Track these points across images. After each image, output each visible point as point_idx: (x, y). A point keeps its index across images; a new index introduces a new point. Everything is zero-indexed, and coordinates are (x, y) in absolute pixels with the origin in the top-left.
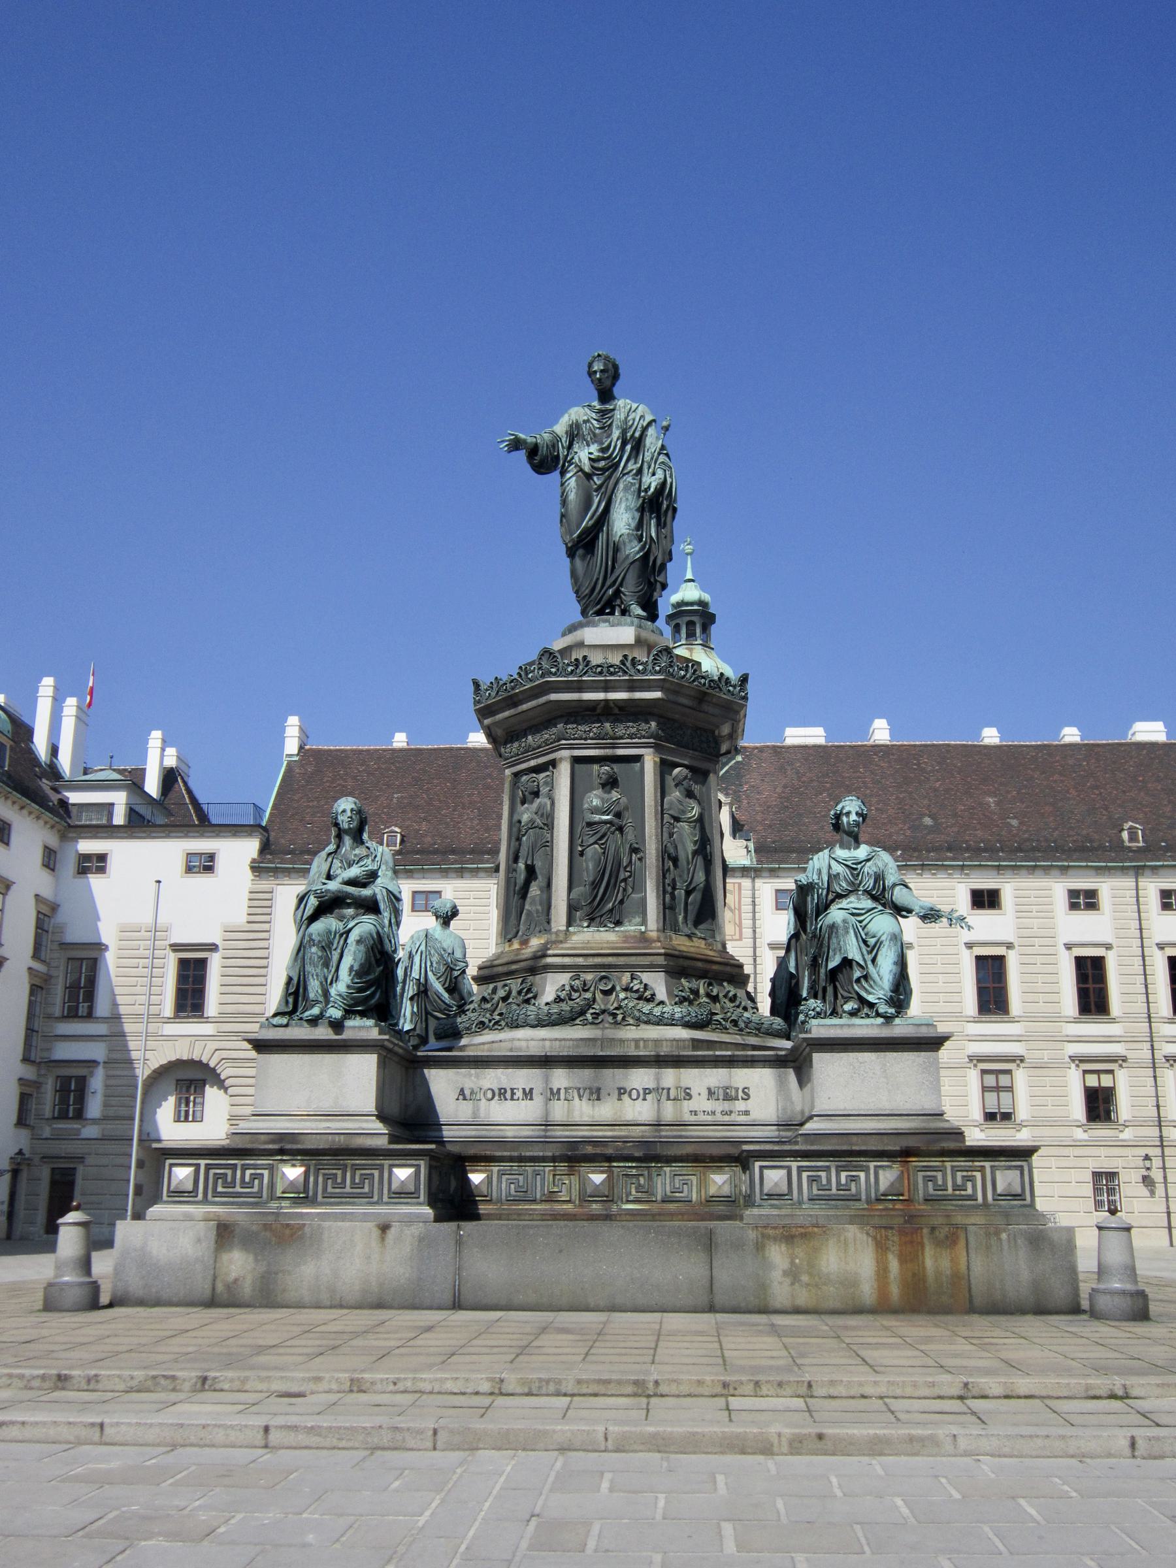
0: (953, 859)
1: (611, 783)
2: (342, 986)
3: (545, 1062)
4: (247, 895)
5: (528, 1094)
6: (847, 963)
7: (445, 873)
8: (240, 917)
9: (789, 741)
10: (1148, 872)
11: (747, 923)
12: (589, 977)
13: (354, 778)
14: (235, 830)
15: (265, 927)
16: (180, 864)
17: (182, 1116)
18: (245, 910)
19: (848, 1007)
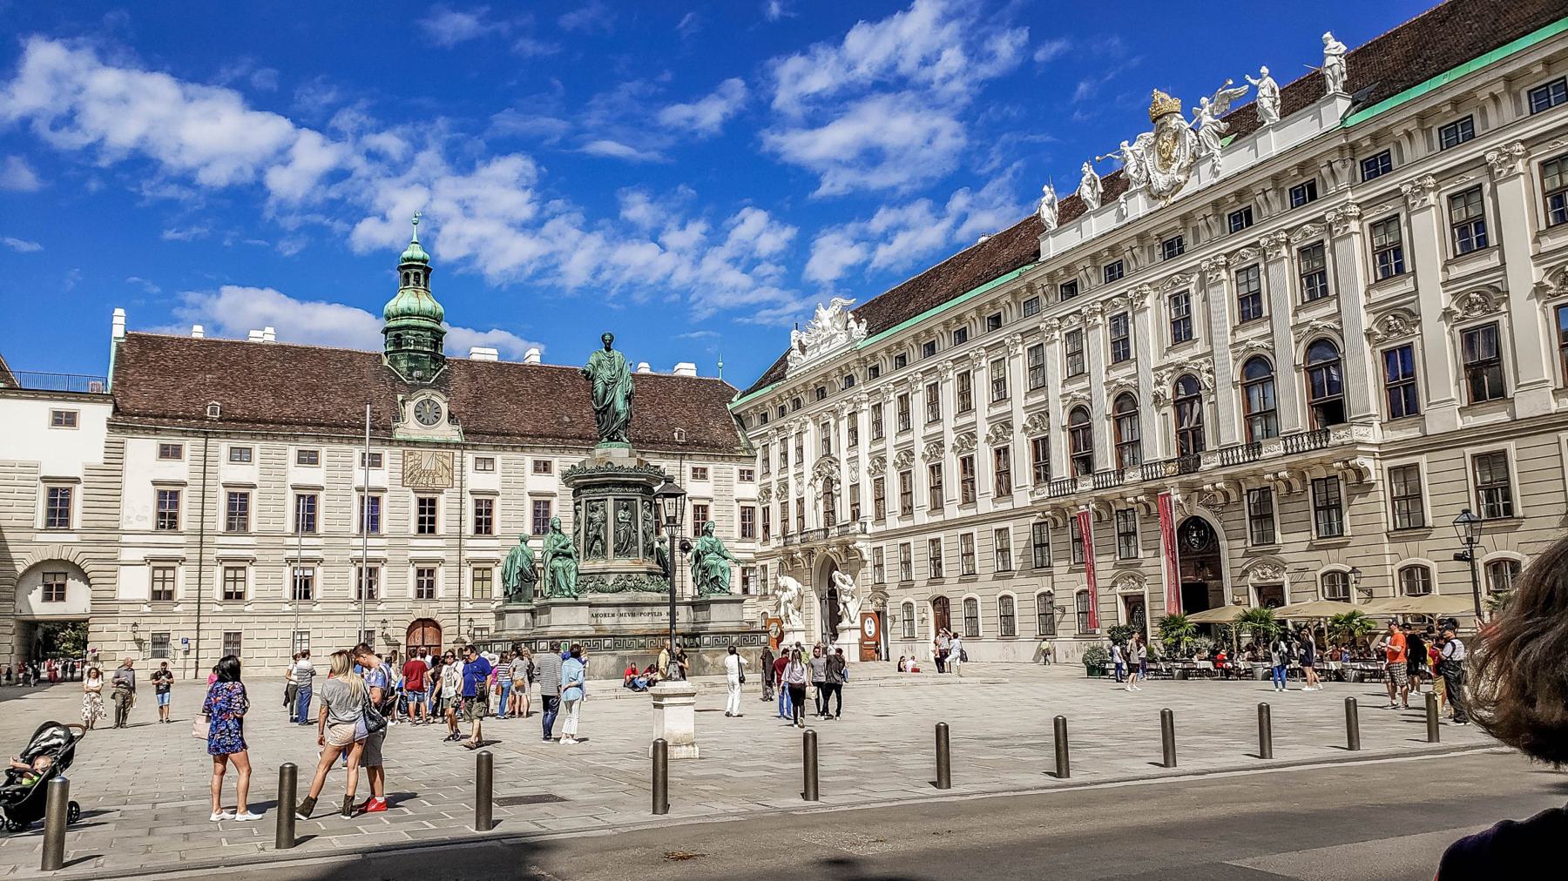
0: (583, 444)
1: (626, 509)
2: (572, 585)
3: (618, 605)
4: (103, 444)
5: (613, 615)
6: (717, 577)
7: (253, 436)
8: (98, 458)
9: (474, 357)
10: (687, 457)
11: (457, 477)
12: (623, 575)
13: (172, 360)
14: (94, 397)
15: (119, 467)
16: (47, 418)
17: (47, 598)
18: (103, 455)
19: (717, 589)
